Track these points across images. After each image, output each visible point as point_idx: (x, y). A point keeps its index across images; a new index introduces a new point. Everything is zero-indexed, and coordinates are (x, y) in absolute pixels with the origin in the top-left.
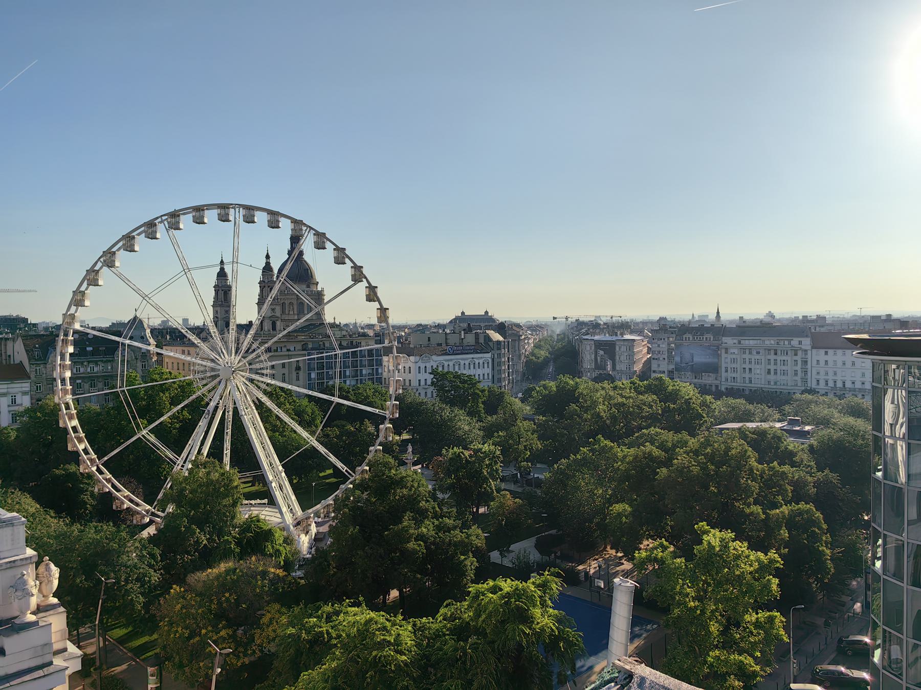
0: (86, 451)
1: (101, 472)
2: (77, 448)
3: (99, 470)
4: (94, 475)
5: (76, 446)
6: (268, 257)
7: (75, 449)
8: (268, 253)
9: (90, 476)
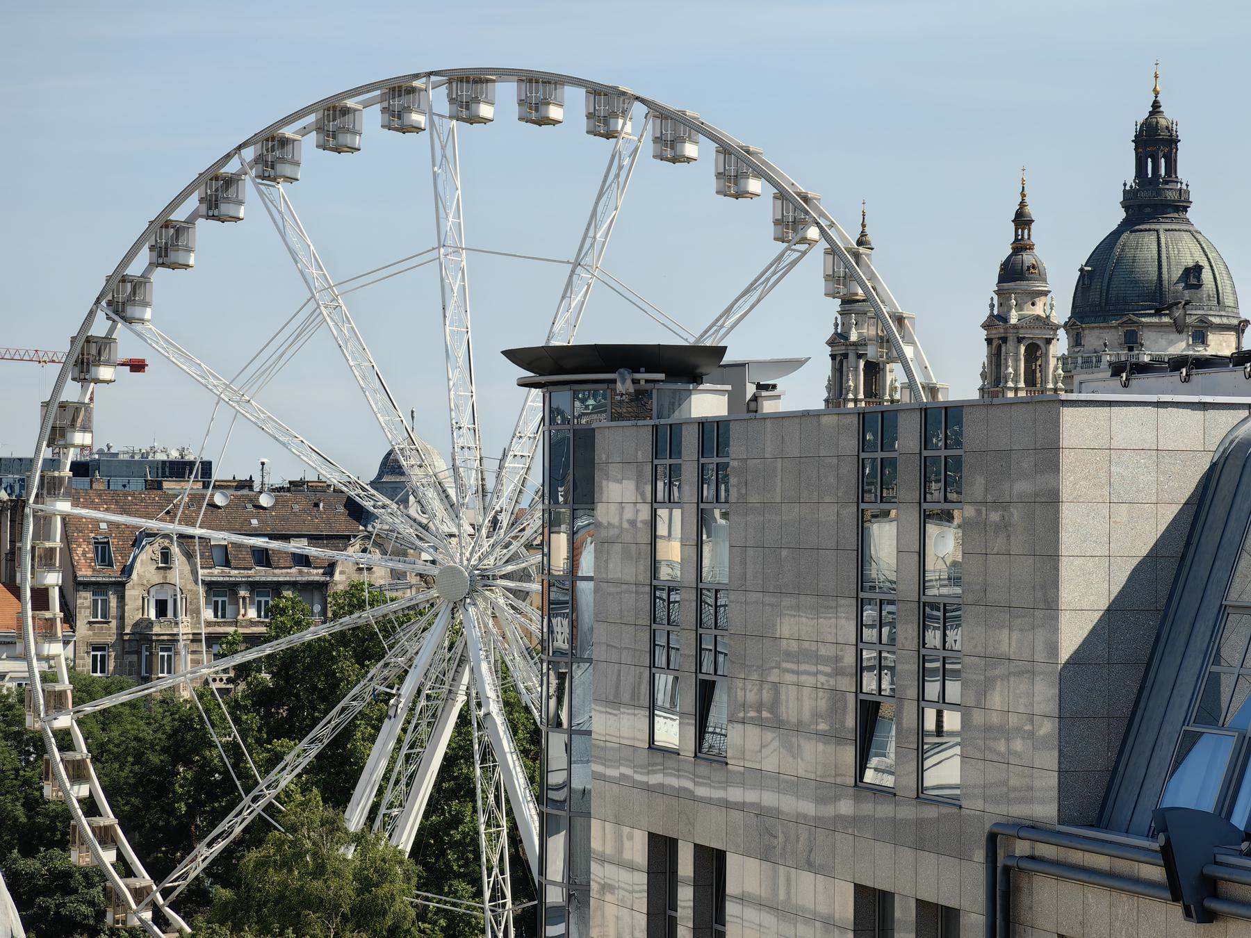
0: (91, 807)
1: (128, 872)
2: (67, 793)
3: (122, 862)
4: (104, 877)
5: (62, 787)
6: (1022, 220)
7: (60, 794)
8: (1022, 204)
9: (94, 875)
